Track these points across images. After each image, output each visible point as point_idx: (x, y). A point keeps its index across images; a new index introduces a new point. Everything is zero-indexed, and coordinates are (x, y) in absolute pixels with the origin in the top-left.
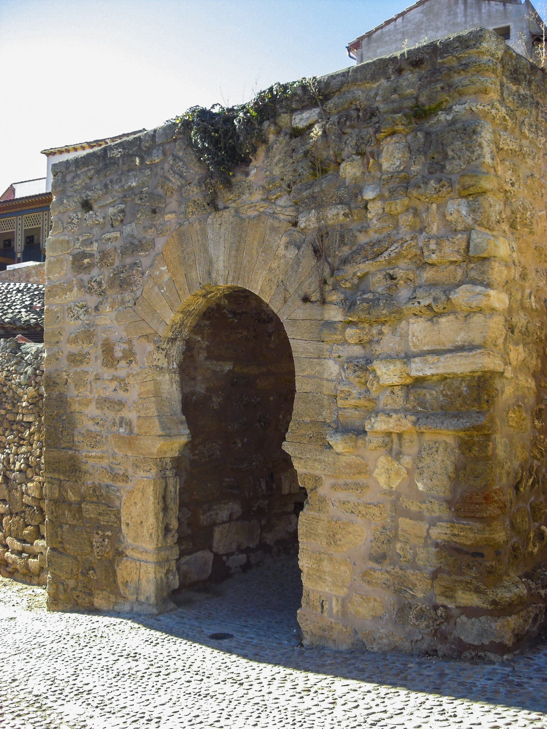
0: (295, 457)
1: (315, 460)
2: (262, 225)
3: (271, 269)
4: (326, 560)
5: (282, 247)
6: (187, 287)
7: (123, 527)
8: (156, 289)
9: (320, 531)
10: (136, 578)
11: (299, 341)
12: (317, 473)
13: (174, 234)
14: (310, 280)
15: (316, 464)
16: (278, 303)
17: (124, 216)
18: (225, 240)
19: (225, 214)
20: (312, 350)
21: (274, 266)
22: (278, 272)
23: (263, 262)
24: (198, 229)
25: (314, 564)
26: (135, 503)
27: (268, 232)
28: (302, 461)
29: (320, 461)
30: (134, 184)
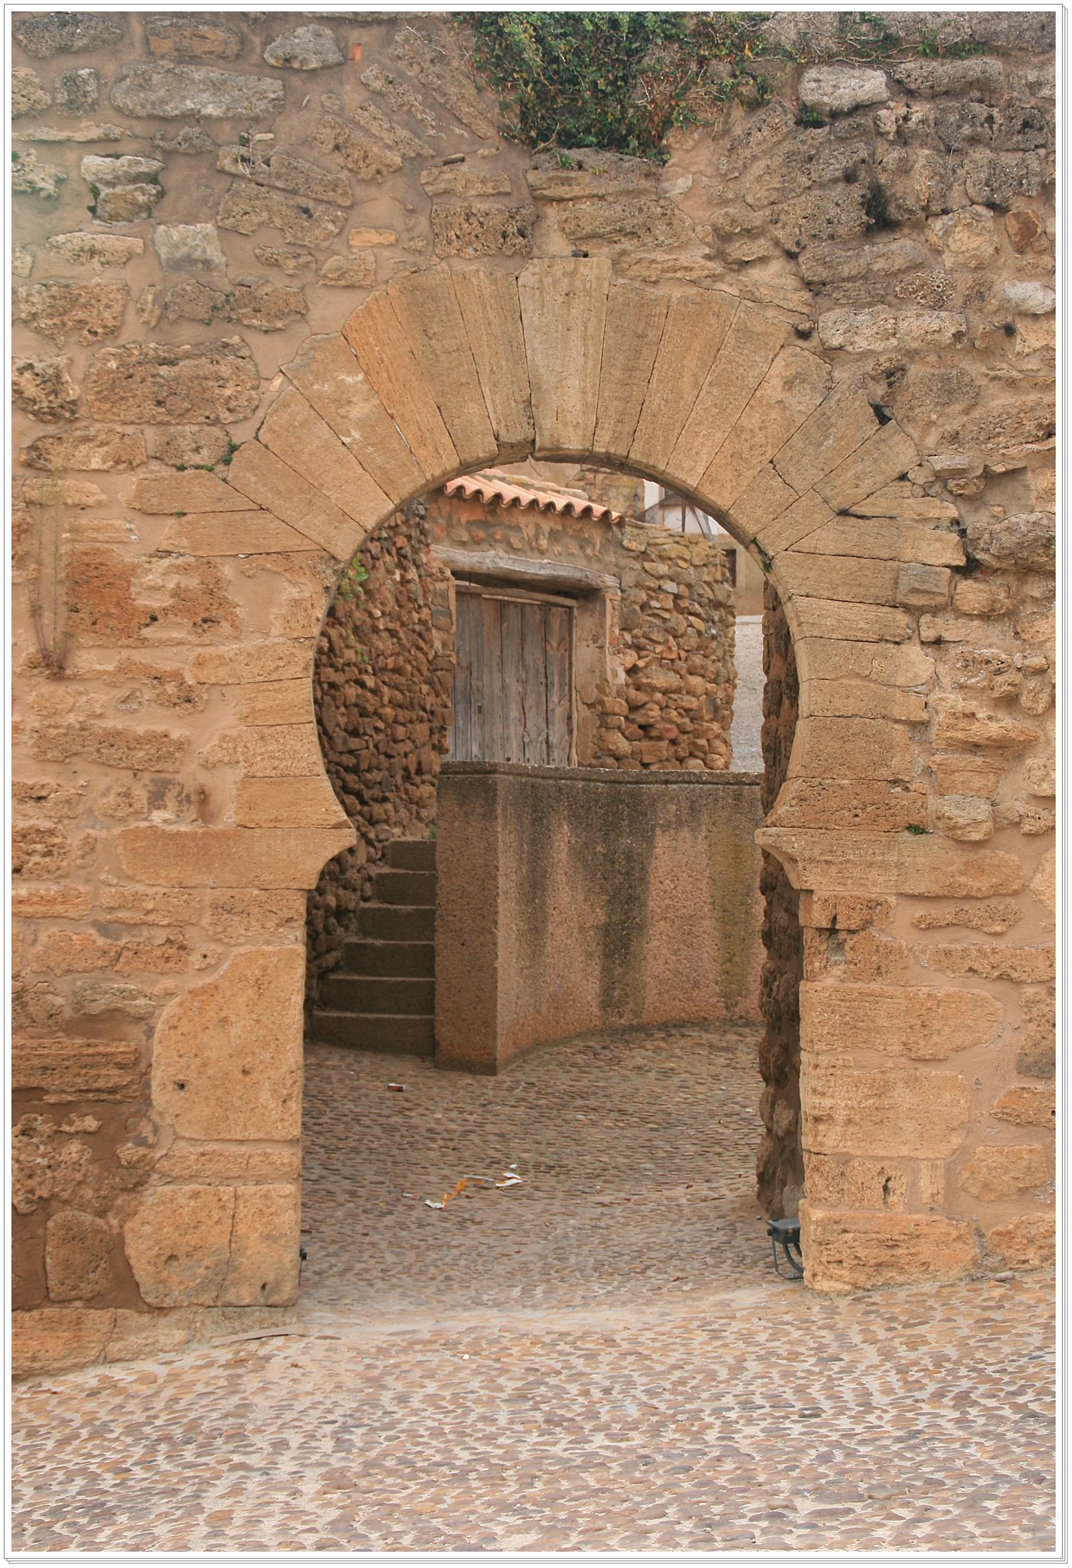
0: (811, 860)
1: (871, 865)
2: (713, 320)
3: (738, 430)
4: (900, 1084)
5: (776, 382)
6: (446, 440)
7: (161, 1097)
8: (325, 432)
9: (882, 1021)
10: (217, 1238)
11: (823, 602)
12: (874, 892)
13: (393, 292)
14: (859, 467)
15: (874, 874)
16: (759, 512)
17: (162, 194)
18: (584, 338)
19: (582, 270)
20: (862, 625)
21: (752, 421)
22: (760, 438)
23: (715, 411)
24: (486, 293)
25: (867, 1097)
26: (224, 1021)
27: (730, 339)
28: (833, 870)
29: (884, 866)
30: (210, 110)
